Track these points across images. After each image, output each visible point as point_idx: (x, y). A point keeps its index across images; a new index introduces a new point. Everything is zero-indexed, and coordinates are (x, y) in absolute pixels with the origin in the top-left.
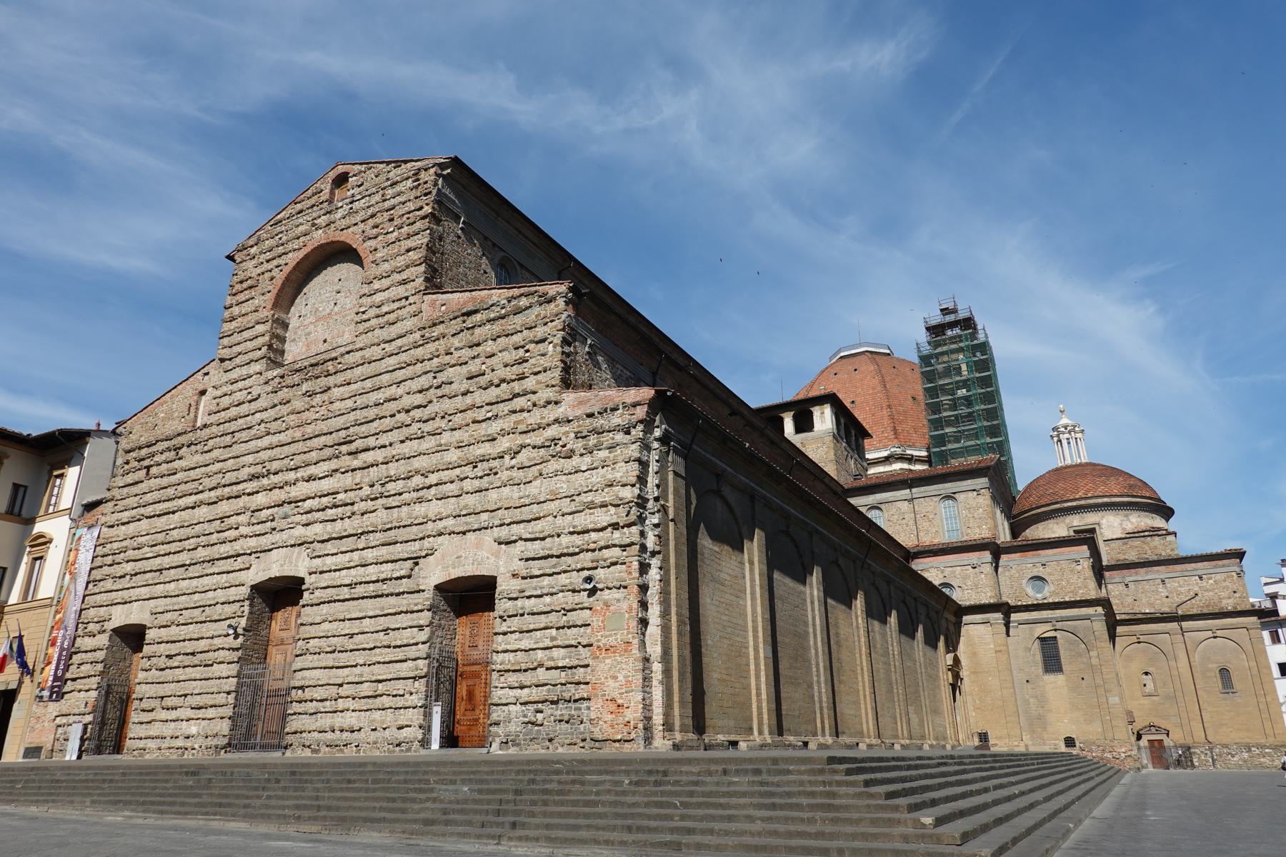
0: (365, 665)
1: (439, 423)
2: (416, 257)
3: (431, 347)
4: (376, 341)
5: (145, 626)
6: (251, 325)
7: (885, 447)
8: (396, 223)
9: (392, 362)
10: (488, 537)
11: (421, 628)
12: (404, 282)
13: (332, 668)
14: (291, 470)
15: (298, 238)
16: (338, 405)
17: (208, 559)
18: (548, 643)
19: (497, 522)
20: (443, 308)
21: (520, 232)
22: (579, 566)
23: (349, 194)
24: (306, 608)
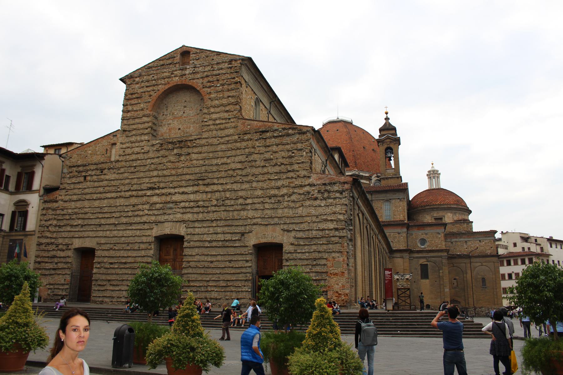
0: (220, 273)
1: (250, 178)
2: (233, 101)
3: (244, 144)
4: (214, 136)
5: (95, 249)
6: (140, 116)
7: (350, 170)
8: (221, 83)
9: (223, 147)
10: (278, 228)
11: (247, 261)
12: (227, 111)
13: (204, 274)
14: (172, 188)
15: (164, 79)
16: (195, 162)
17: (128, 222)
18: (308, 270)
19: (282, 222)
20: (249, 127)
21: (262, 86)
22: (321, 242)
23: (191, 62)
24: (186, 249)
